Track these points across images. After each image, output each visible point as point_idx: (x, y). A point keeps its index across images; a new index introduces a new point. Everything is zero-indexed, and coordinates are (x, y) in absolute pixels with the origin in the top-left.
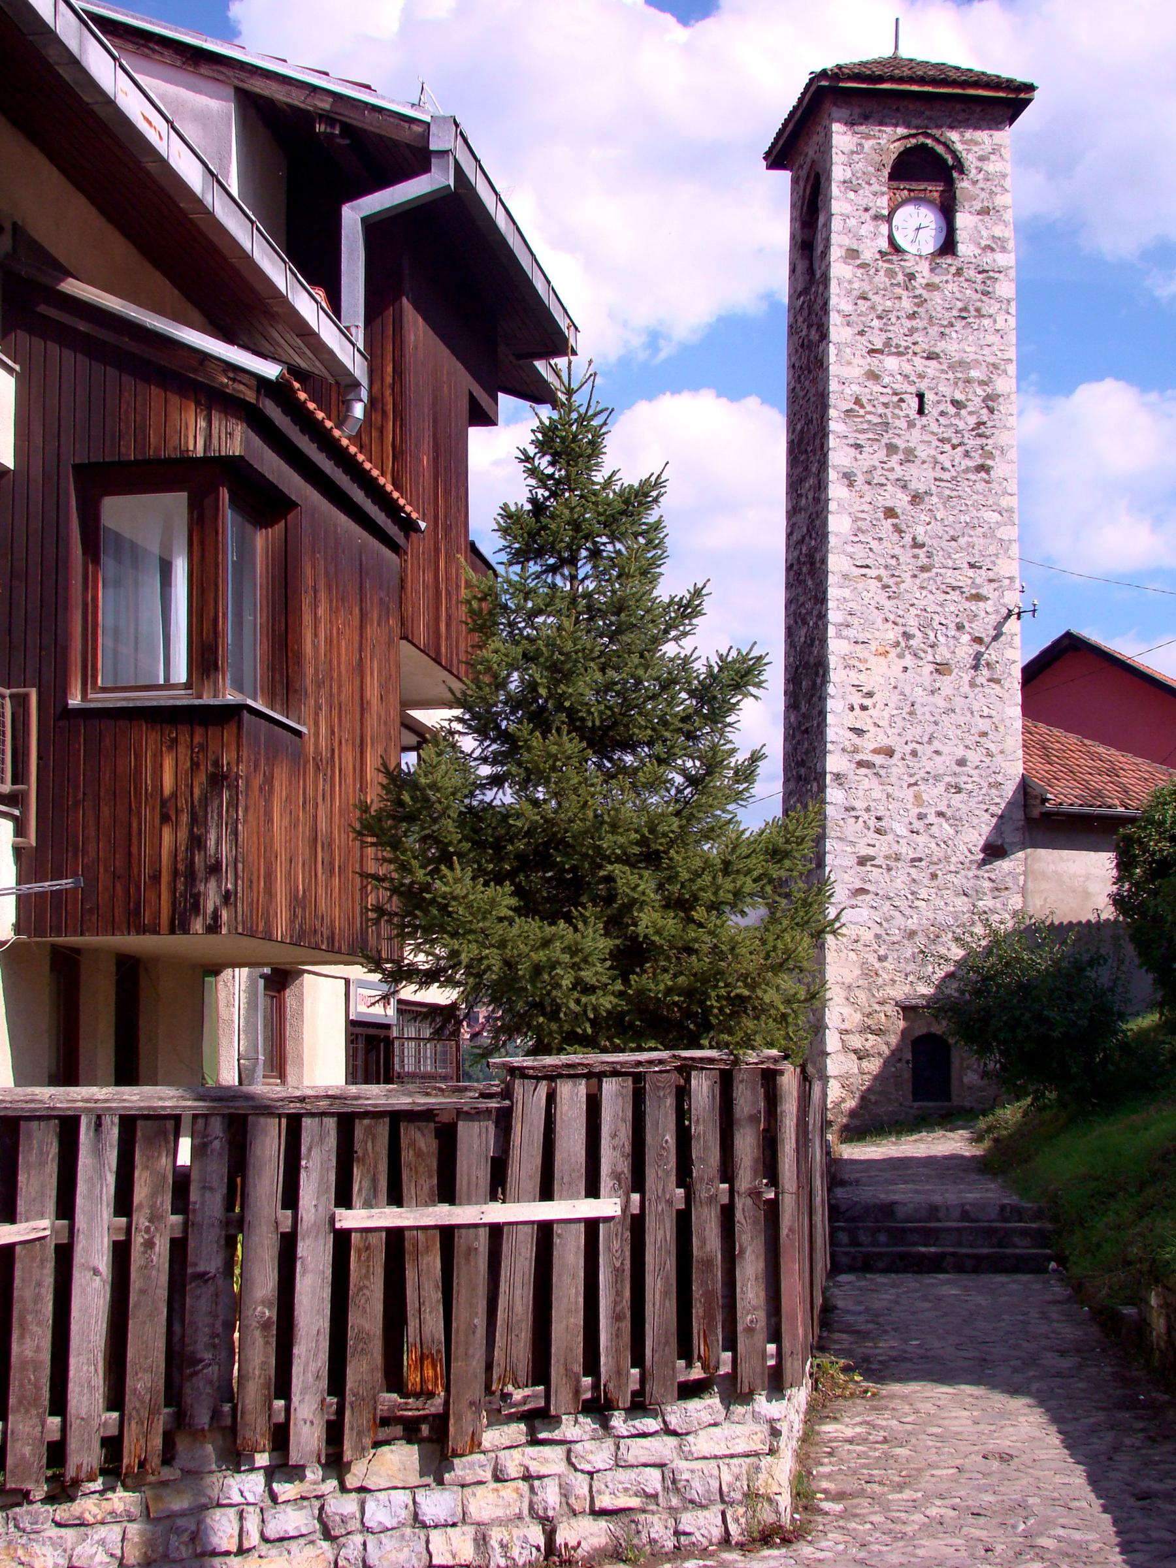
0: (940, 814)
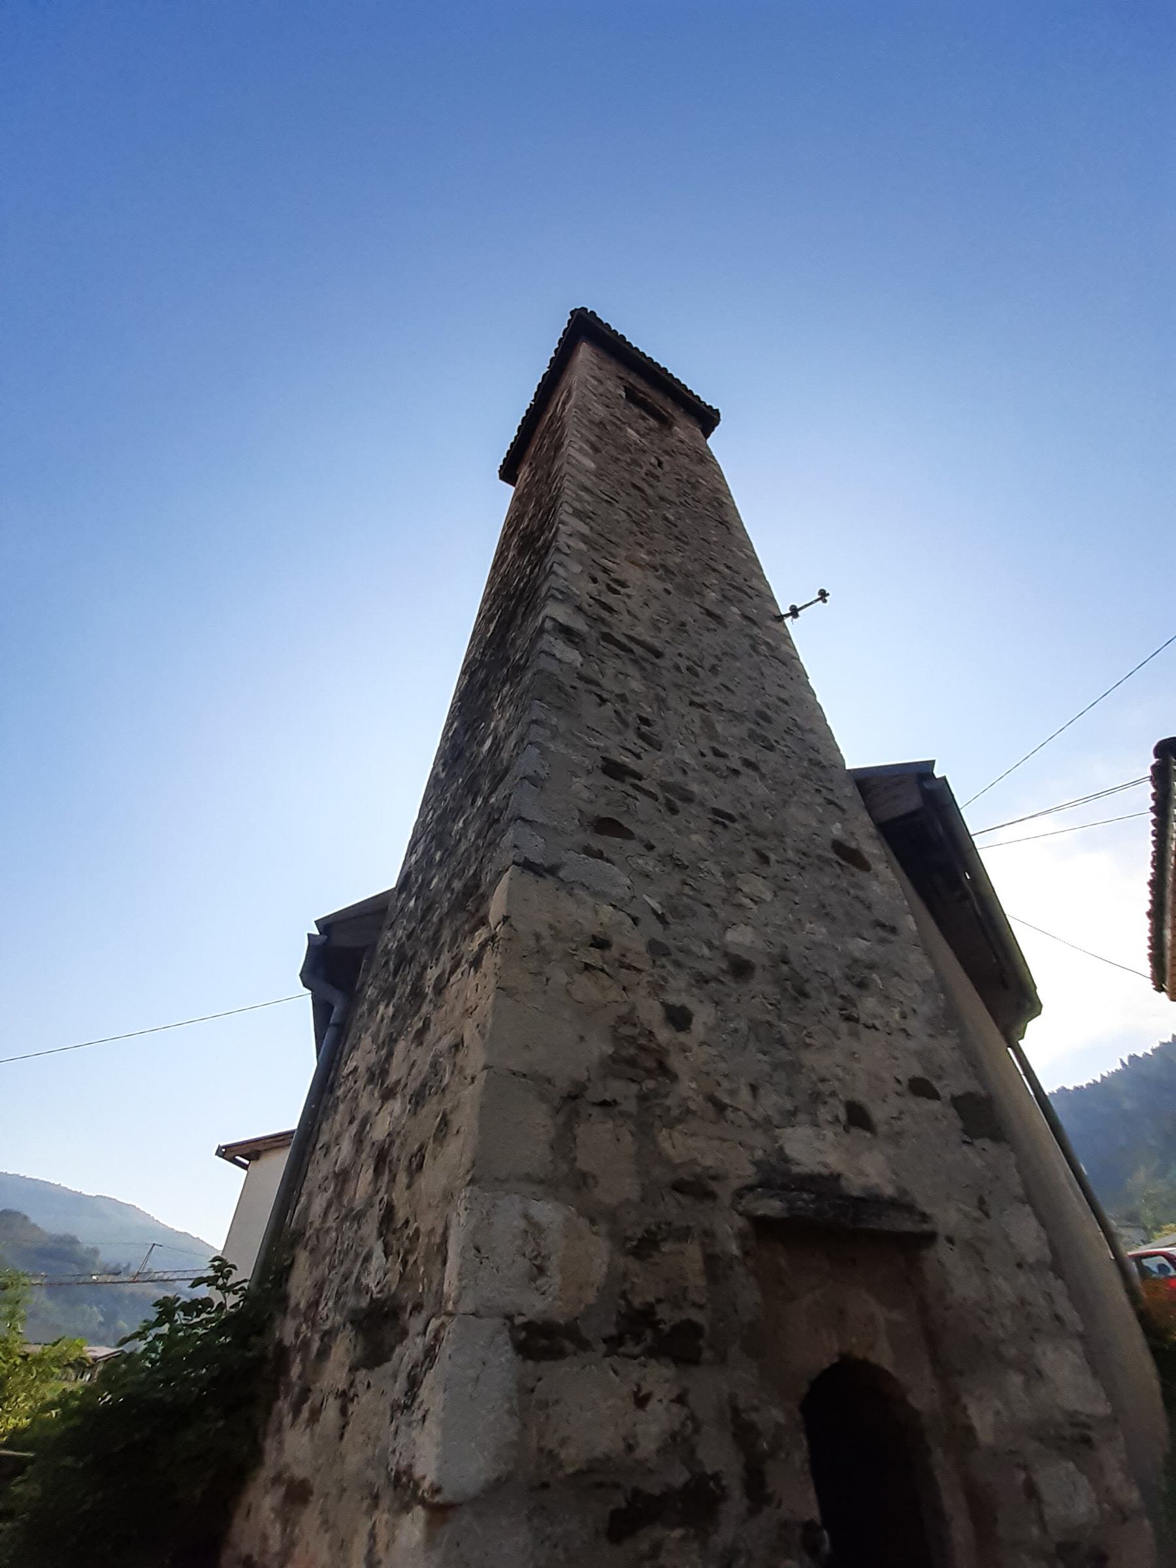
0: (748, 763)
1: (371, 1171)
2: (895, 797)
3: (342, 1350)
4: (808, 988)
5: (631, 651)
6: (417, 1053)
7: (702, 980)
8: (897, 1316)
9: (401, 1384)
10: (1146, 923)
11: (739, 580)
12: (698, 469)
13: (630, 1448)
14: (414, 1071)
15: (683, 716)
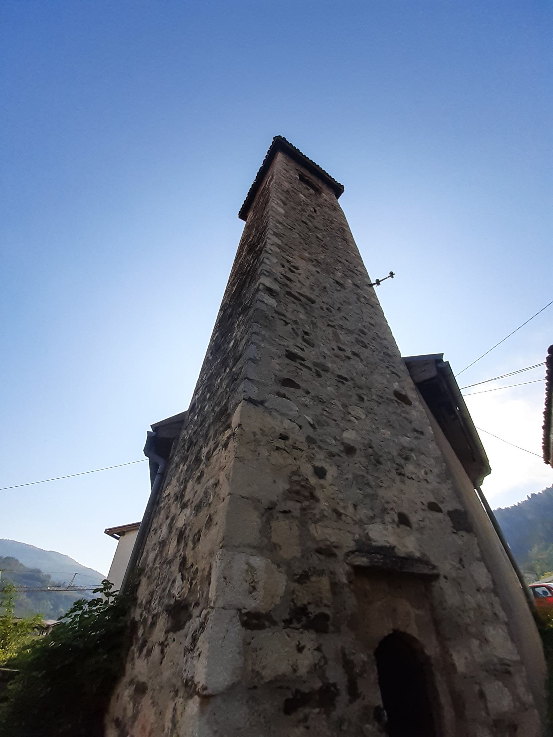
0: (354, 354)
1: (175, 543)
2: (424, 371)
3: (162, 623)
4: (381, 459)
5: (300, 300)
6: (198, 487)
7: (331, 455)
8: (420, 612)
9: (189, 639)
10: (541, 432)
11: (352, 266)
12: (333, 213)
13: (295, 671)
14: (196, 496)
15: (324, 331)
